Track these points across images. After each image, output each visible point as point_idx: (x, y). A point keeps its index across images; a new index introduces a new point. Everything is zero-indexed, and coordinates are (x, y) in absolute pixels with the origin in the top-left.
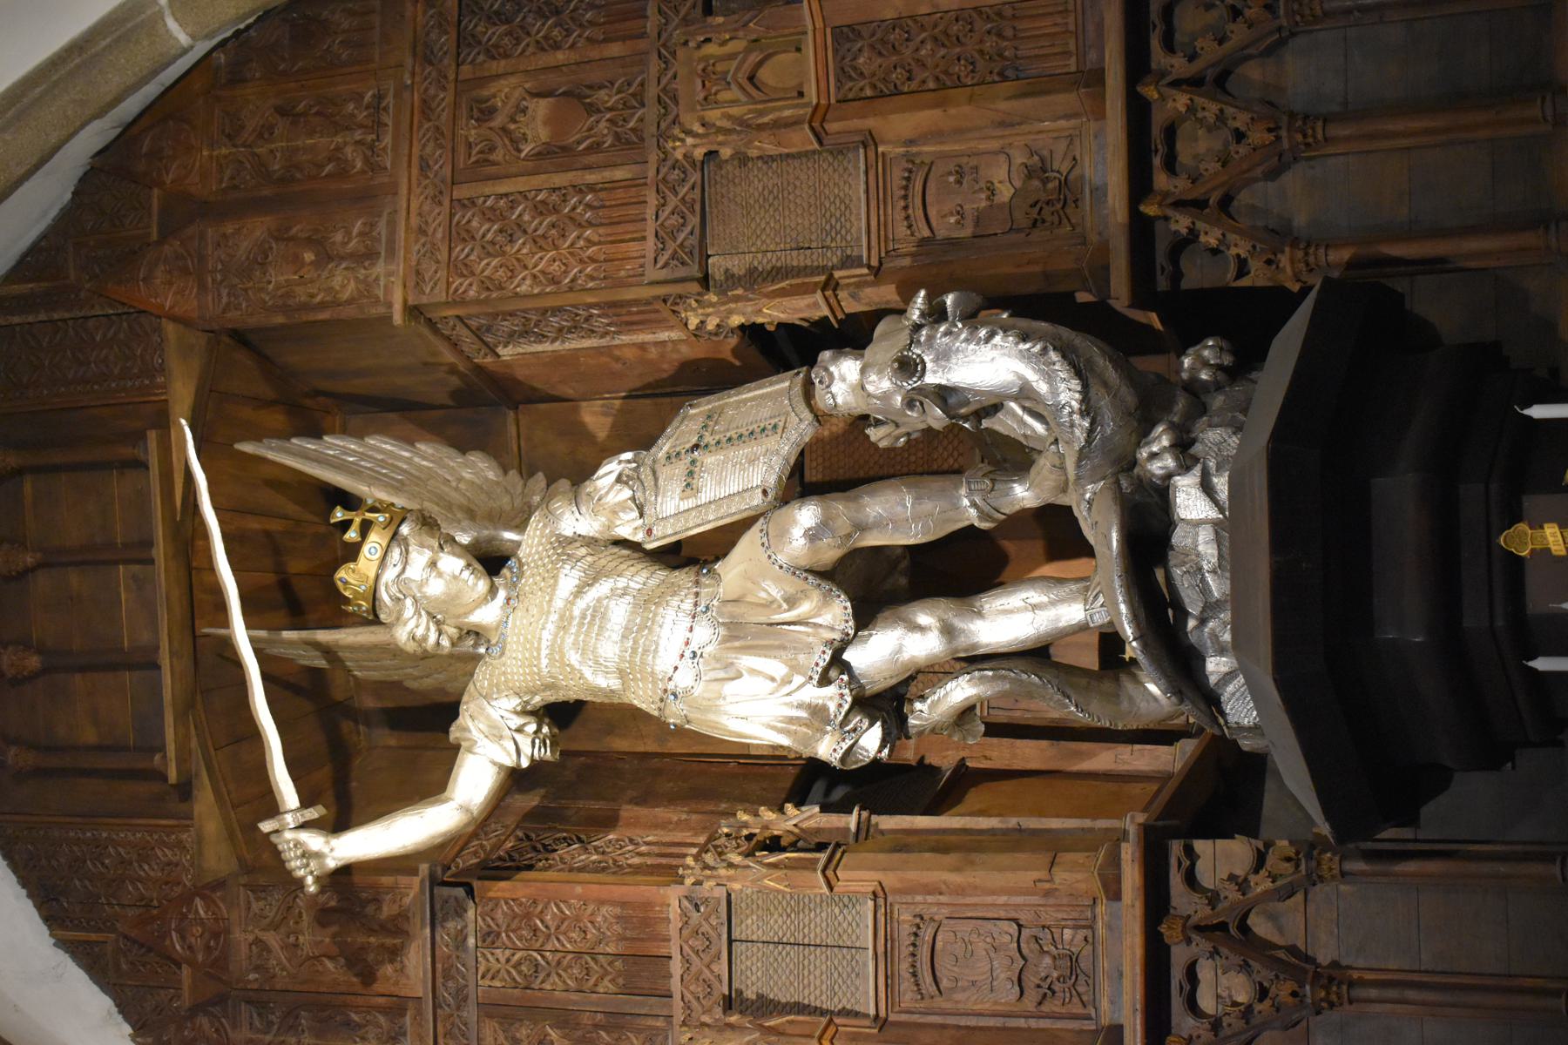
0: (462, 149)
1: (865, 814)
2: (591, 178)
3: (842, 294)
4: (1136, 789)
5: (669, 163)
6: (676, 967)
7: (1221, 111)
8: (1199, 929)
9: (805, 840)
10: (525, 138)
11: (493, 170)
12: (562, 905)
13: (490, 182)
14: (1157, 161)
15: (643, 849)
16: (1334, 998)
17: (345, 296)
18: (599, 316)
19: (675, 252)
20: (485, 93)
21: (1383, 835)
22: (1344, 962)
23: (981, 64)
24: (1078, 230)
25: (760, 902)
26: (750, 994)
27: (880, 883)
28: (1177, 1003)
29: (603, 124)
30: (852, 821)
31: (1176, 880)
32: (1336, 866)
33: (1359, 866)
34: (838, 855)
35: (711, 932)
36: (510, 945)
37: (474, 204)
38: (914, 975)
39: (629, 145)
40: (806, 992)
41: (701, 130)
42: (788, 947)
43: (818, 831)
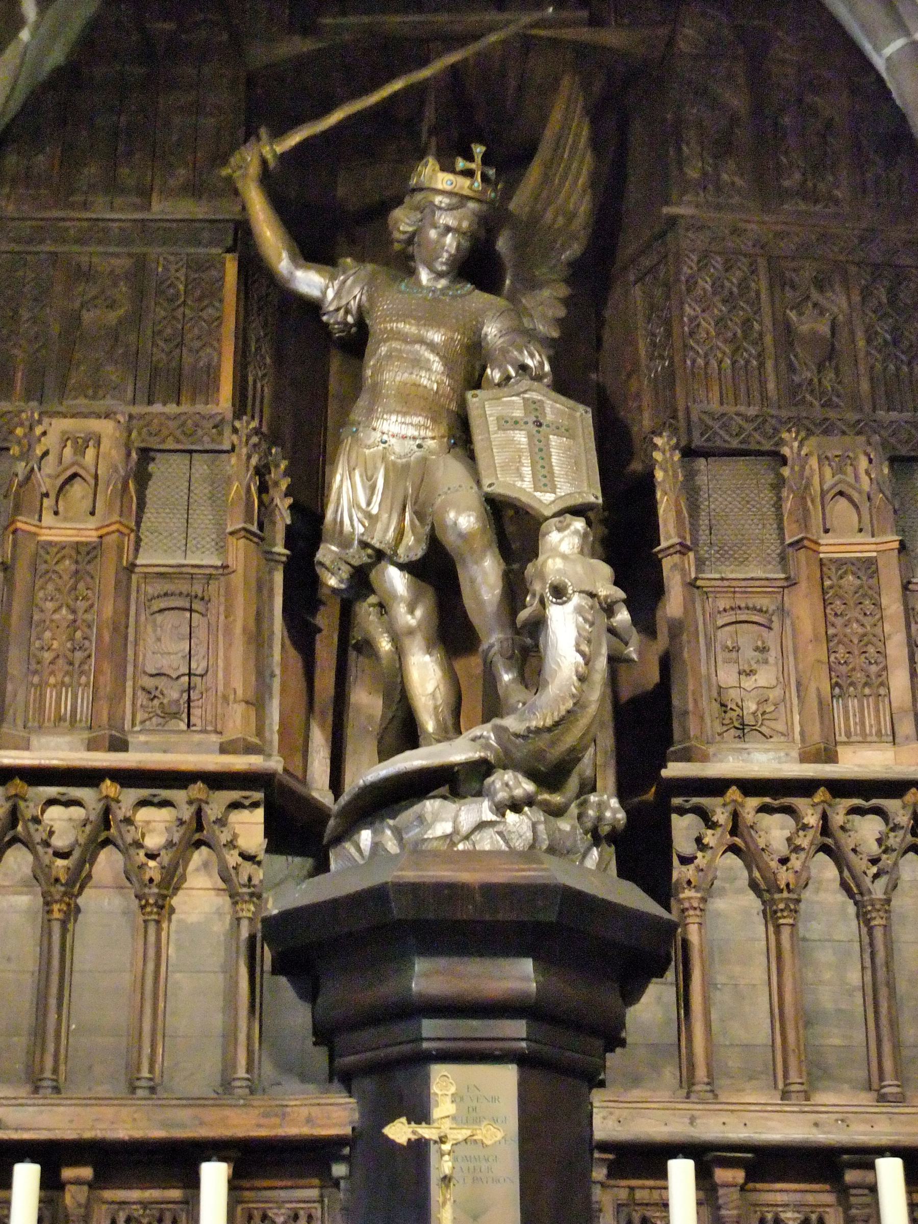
0: (794, 264)
1: (284, 559)
3: (676, 558)
5: (778, 426)
6: (172, 409)
7: (803, 849)
8: (199, 813)
10: (801, 314)
14: (767, 800)
15: (259, 385)
16: (148, 909)
17: (686, 170)
20: (837, 287)
21: (266, 948)
22: (174, 917)
23: (844, 669)
24: (718, 738)
26: (151, 467)
27: (233, 572)
28: (144, 793)
30: (280, 548)
31: (235, 795)
32: (245, 914)
33: (245, 933)
34: (256, 540)
37: (753, 272)
38: (166, 594)
39: (792, 393)
41: (803, 453)
43: (274, 523)
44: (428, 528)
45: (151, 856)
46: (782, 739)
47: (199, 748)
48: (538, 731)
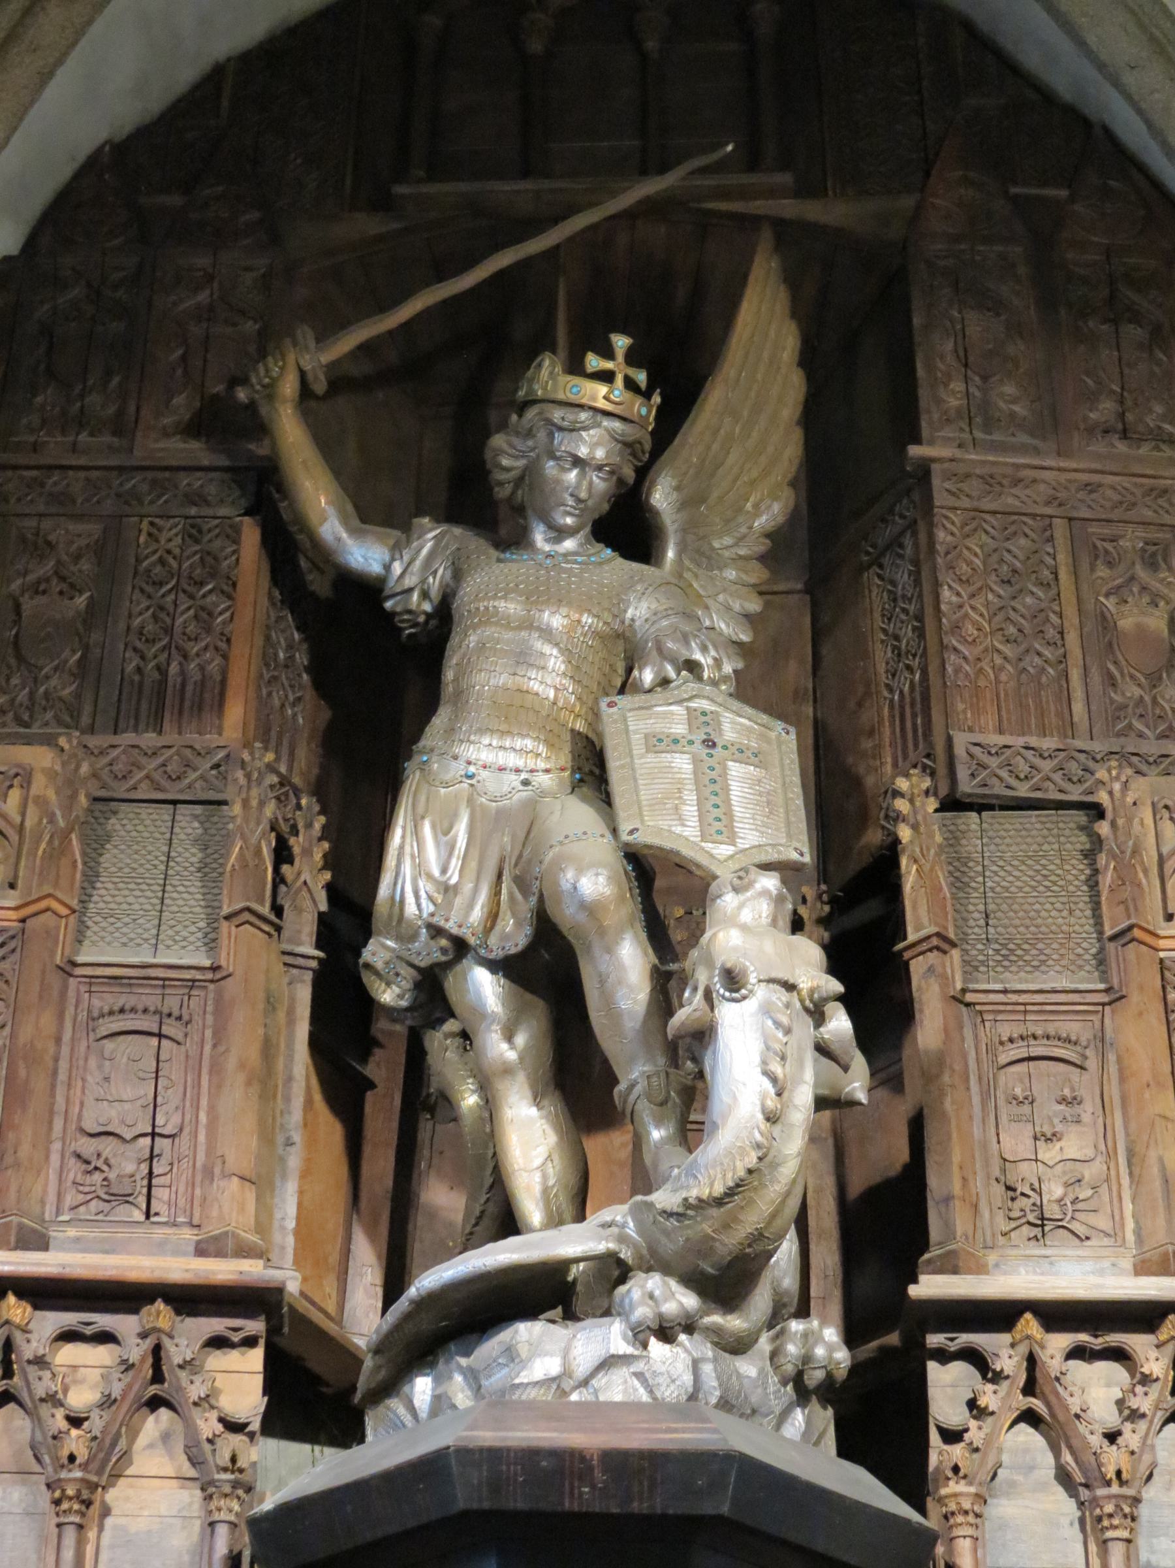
0: (1106, 531)
1: (314, 964)
2: (1075, 675)
3: (933, 957)
4: (330, 1286)
5: (1091, 764)
6: (149, 739)
7: (1143, 1416)
8: (157, 1350)
9: (287, 893)
11: (1085, 566)
12: (228, 614)
13: (1070, 560)
14: (1083, 1337)
16: (65, 1506)
18: (912, 682)
19: (985, 767)
22: (109, 1522)
24: (1001, 1240)
25: (217, 838)
27: (229, 975)
29: (1137, 692)
31: (216, 1325)
32: (223, 1516)
34: (266, 928)
35: (187, 781)
36: (185, 554)
40: (110, 886)
41: (1129, 800)
42: (163, 867)
44: (533, 900)
45: (76, 1421)
46: (1106, 1241)
47: (161, 1248)
48: (702, 1204)
